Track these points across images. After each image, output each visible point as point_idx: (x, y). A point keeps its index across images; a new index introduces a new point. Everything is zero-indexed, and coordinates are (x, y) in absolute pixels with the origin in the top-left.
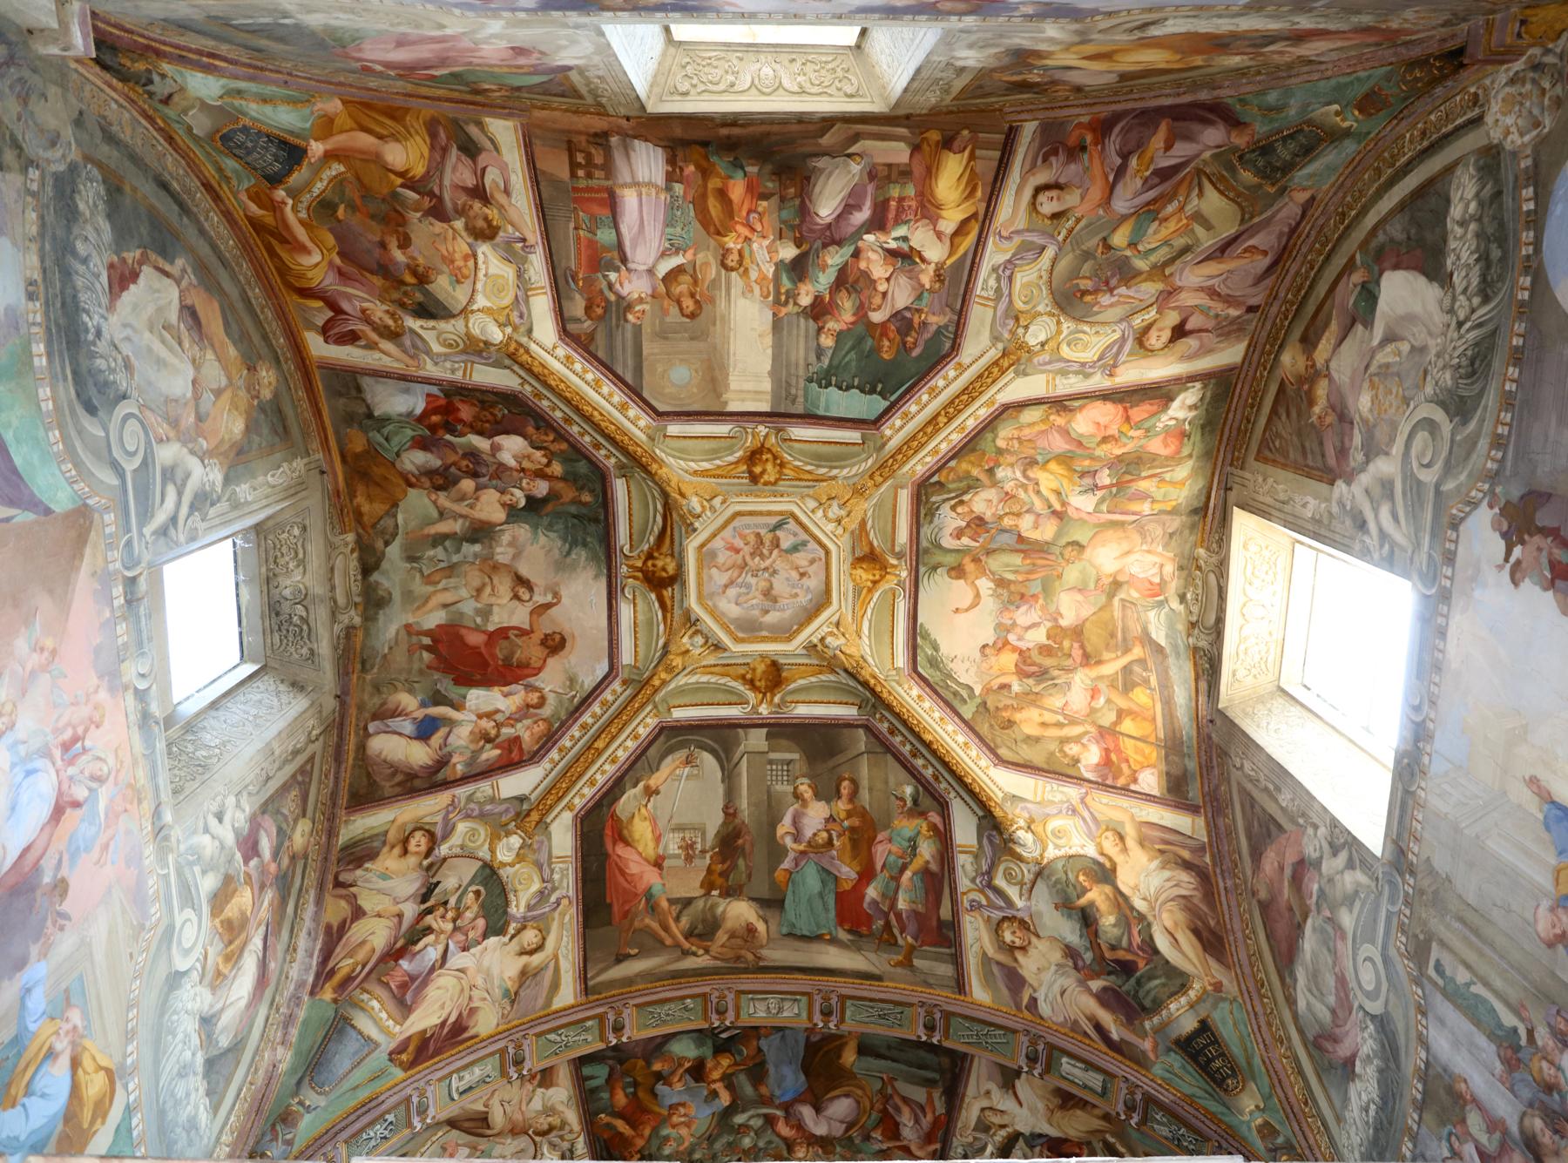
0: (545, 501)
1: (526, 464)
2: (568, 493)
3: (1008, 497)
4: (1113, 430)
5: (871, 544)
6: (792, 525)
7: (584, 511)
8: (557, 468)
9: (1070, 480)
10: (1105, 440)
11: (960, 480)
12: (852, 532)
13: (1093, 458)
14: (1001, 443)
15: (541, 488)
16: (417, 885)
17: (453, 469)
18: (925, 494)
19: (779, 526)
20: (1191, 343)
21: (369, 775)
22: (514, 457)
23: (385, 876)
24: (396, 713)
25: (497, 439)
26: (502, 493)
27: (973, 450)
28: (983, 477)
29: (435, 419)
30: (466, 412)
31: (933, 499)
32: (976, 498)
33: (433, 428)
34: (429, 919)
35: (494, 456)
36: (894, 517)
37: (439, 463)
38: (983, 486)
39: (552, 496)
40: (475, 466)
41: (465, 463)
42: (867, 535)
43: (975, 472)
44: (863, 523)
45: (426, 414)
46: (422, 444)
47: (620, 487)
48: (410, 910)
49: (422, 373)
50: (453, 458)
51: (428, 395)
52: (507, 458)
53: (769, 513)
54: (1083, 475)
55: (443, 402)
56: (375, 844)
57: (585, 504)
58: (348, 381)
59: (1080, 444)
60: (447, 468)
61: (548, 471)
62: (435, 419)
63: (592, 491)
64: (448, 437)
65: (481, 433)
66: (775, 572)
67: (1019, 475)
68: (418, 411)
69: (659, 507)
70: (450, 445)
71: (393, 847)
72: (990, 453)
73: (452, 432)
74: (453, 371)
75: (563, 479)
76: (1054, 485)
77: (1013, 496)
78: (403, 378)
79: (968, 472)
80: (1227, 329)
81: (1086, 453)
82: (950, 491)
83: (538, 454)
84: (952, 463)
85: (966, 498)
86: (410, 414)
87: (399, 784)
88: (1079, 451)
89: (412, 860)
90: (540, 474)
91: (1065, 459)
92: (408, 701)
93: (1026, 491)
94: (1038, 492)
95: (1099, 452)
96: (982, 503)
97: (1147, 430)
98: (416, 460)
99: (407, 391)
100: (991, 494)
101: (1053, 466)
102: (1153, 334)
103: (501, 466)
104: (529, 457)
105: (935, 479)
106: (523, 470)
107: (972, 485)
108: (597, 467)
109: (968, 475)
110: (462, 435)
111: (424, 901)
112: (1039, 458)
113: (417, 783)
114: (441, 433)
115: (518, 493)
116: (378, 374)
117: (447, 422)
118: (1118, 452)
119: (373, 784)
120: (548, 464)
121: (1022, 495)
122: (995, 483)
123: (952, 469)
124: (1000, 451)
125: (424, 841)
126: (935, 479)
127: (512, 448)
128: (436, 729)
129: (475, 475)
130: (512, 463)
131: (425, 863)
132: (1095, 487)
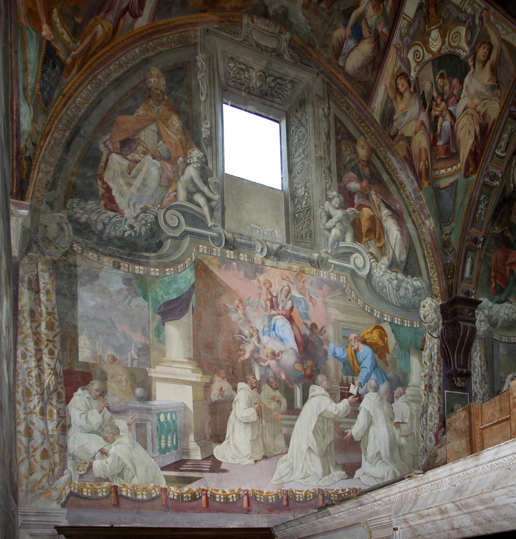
16: (417, 102)
21: (360, 82)
23: (404, 114)
24: (341, 45)
34: (434, 113)
48: (423, 117)
56: (389, 106)
71: (396, 99)
87: (373, 70)
89: (407, 95)
92: (339, 33)
111: (425, 108)
113: (378, 60)
119: (365, 84)
125: (403, 81)
128: (360, 28)
131: (412, 90)
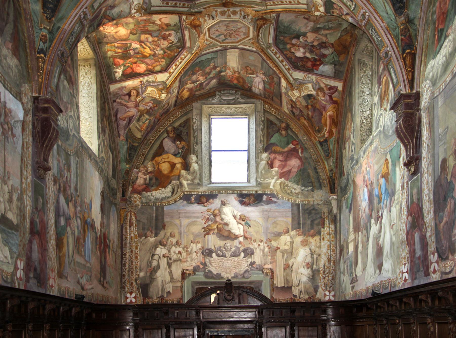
0: (294, 38)
1: (297, 48)
2: (287, 40)
3: (158, 46)
4: (134, 65)
5: (196, 30)
6: (221, 40)
7: (283, 35)
8: (288, 46)
9: (141, 51)
10: (135, 63)
11: (173, 50)
12: (202, 33)
13: (137, 57)
14: (164, 60)
15: (294, 41)
17: (318, 48)
18: (181, 46)
19: (224, 40)
20: (125, 92)
22: (300, 50)
25: (303, 56)
26: (306, 40)
27: (171, 58)
28: (167, 51)
29: (318, 63)
30: (309, 64)
31: (179, 44)
32: (167, 45)
33: (320, 60)
35: (306, 51)
36: (190, 38)
37: (322, 50)
38: (166, 48)
39: (291, 39)
40: (311, 48)
41: (314, 50)
42: (197, 33)
43: (169, 52)
44: (199, 36)
45: (320, 65)
46: (324, 56)
47: (271, 41)
49: (317, 77)
50: (316, 51)
51: (317, 70)
52: (302, 50)
53: (227, 43)
54: (138, 53)
55: (315, 68)
57: (283, 36)
58: (336, 76)
59: (142, 61)
60: (320, 49)
61: (291, 46)
62: (318, 63)
63: (280, 39)
64: (316, 57)
65: (307, 58)
66: (225, 30)
67: (157, 52)
68: (322, 66)
69: (260, 35)
70: (317, 55)
72: (166, 57)
73: (315, 59)
74: (309, 77)
75: (287, 43)
76: (146, 50)
77: (156, 46)
78: (322, 76)
79: (171, 52)
80: (117, 95)
81: (140, 59)
82: (175, 46)
83: (293, 51)
84: (176, 54)
85: (170, 45)
86: (324, 65)
88: (142, 59)
90: (294, 45)
91: (145, 57)
93: (153, 48)
94: (149, 47)
95: (136, 59)
96: (165, 44)
97: (125, 66)
98: (326, 52)
99: (323, 72)
100: (163, 46)
101: (148, 55)
102: (135, 94)
103: (304, 48)
104: (296, 50)
105: (180, 50)
106: (298, 46)
107: (169, 48)
108: (277, 46)
109: (171, 51)
110: (312, 58)
112: (152, 57)
114: (318, 59)
115: (301, 40)
116: (328, 77)
117: (315, 62)
118: (130, 60)
120: (291, 47)
121: (154, 46)
122: (163, 49)
123: (176, 53)
124: (163, 58)
126: (180, 50)
127: (300, 54)
129: (313, 46)
130: (301, 49)
132: (134, 49)
